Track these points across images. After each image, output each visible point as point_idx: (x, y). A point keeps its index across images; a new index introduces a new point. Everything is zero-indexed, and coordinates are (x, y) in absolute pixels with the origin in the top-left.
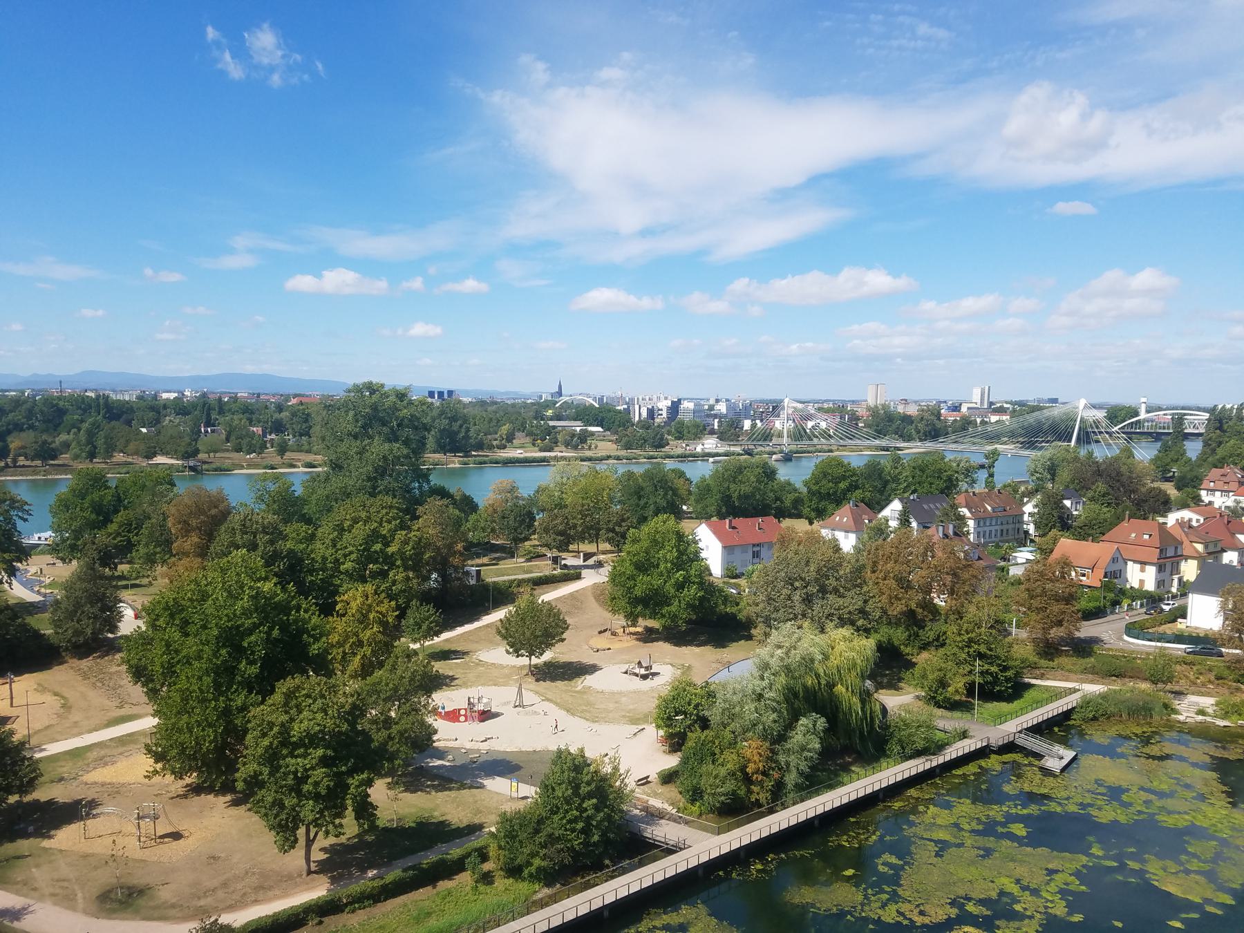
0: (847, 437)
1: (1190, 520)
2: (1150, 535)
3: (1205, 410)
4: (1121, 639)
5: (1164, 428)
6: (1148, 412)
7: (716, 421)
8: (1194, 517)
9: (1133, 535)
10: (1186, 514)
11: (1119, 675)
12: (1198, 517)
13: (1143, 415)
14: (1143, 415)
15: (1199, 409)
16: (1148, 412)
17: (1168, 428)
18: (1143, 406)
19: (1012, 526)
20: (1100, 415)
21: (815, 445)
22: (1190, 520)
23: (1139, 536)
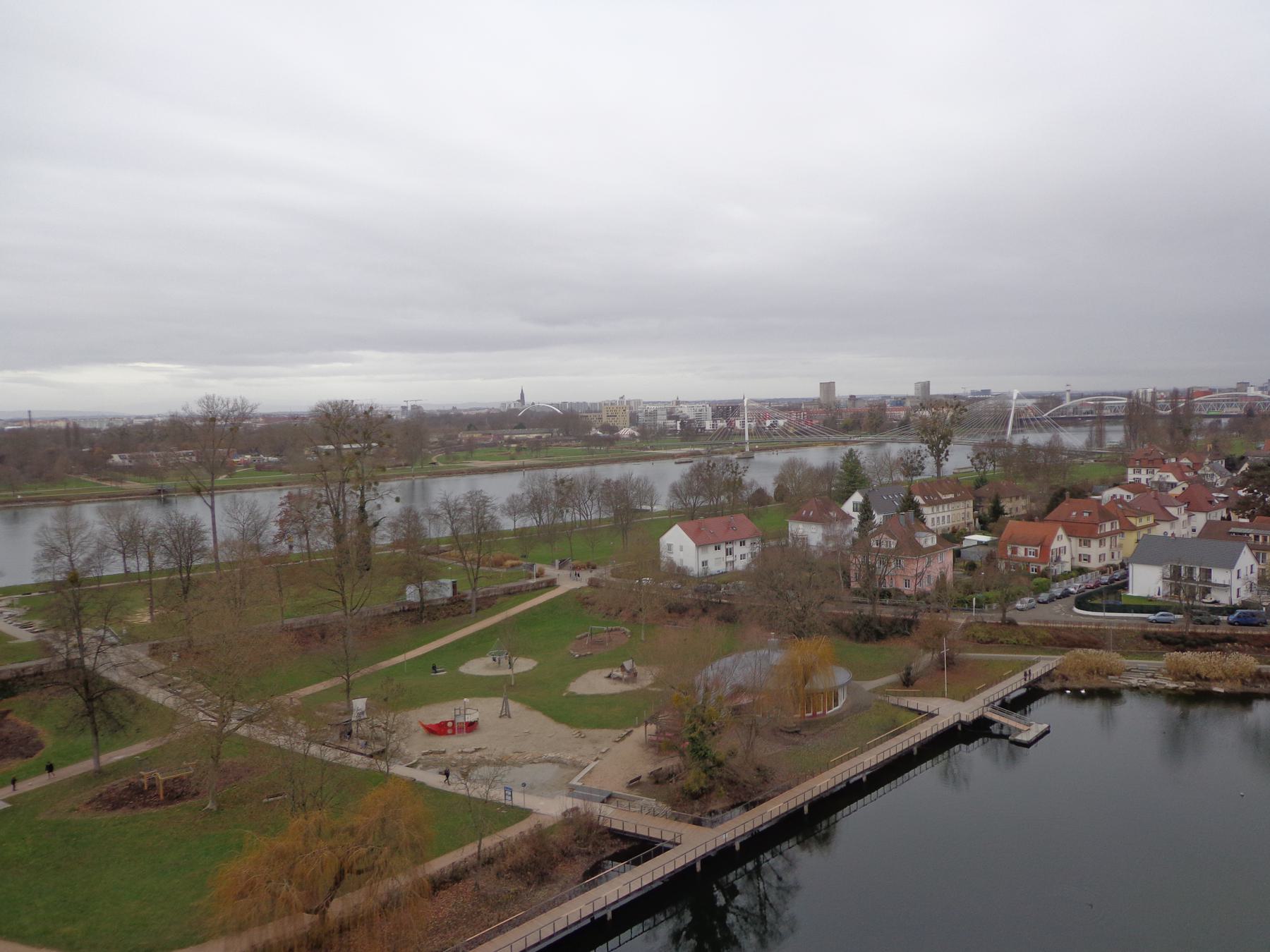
0: (807, 431)
1: (1122, 497)
2: (1090, 513)
3: (1122, 395)
4: (1071, 610)
5: (1088, 413)
6: (1072, 398)
7: (679, 422)
8: (1125, 493)
9: (1074, 514)
10: (1118, 492)
11: (1072, 644)
12: (1129, 494)
13: (1068, 403)
14: (1068, 403)
15: (1116, 394)
16: (1072, 398)
17: (1092, 413)
18: (1068, 394)
19: (963, 511)
20: (1029, 402)
21: (789, 442)
22: (1122, 497)
23: (1080, 514)
